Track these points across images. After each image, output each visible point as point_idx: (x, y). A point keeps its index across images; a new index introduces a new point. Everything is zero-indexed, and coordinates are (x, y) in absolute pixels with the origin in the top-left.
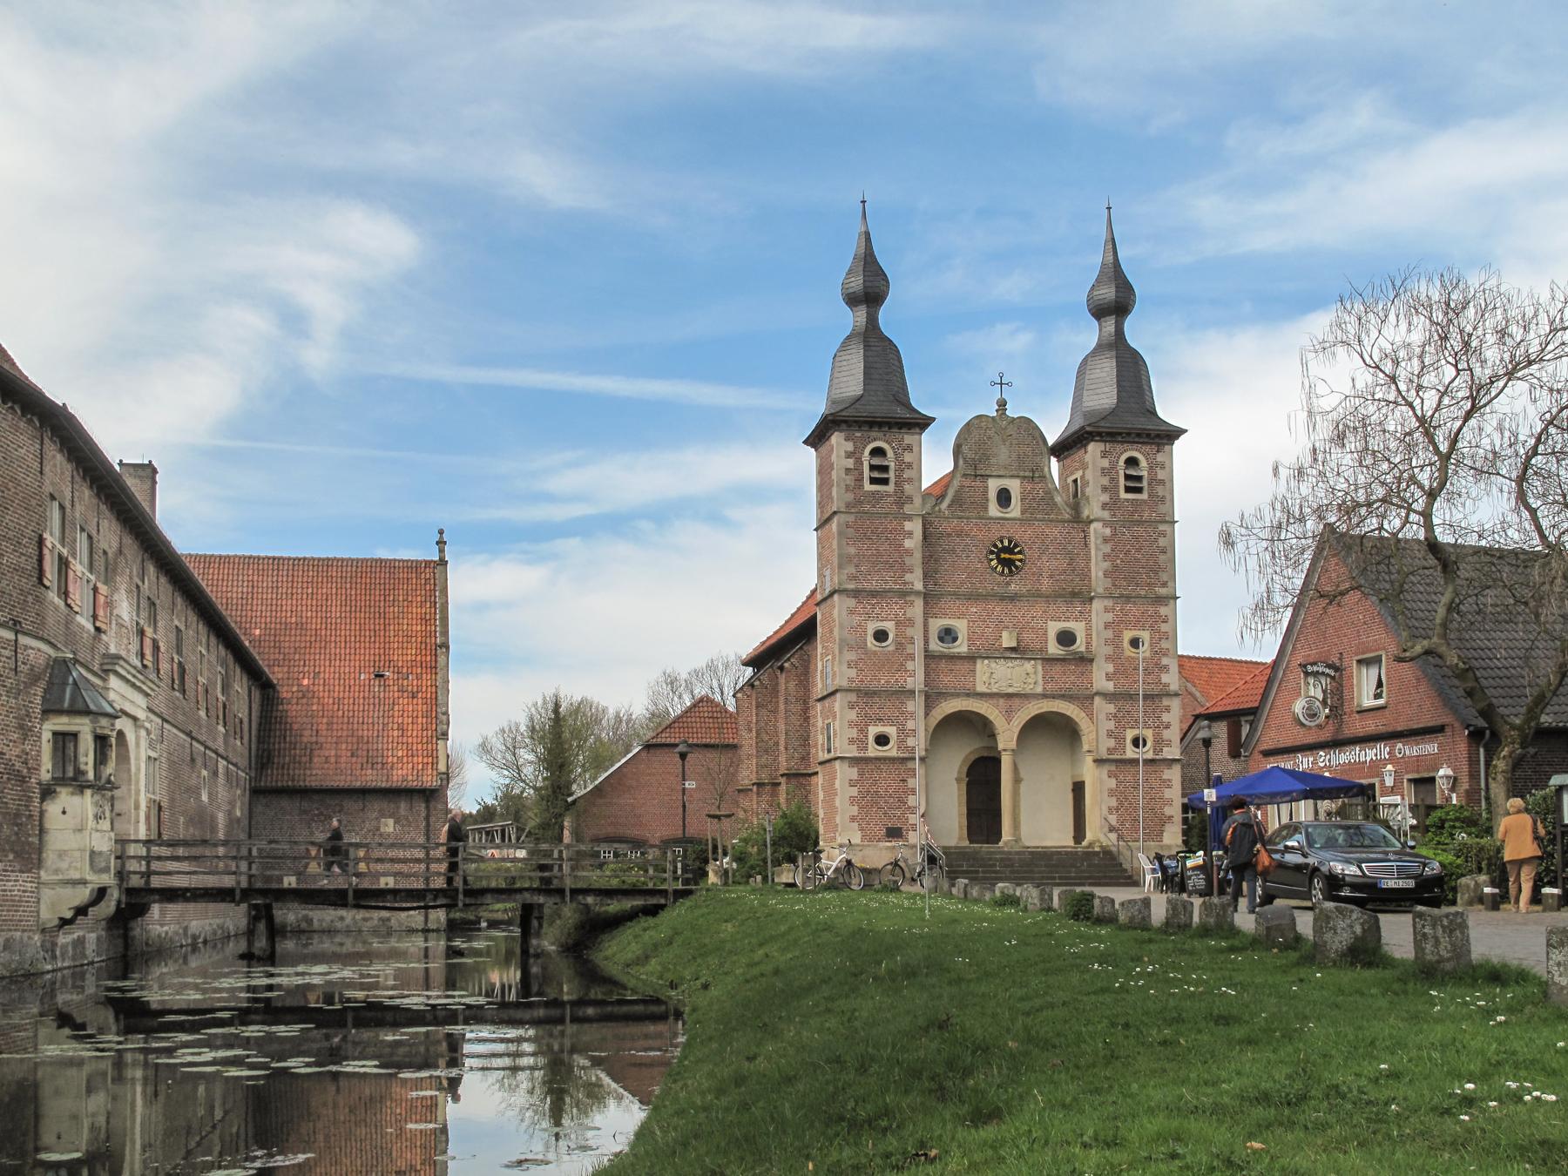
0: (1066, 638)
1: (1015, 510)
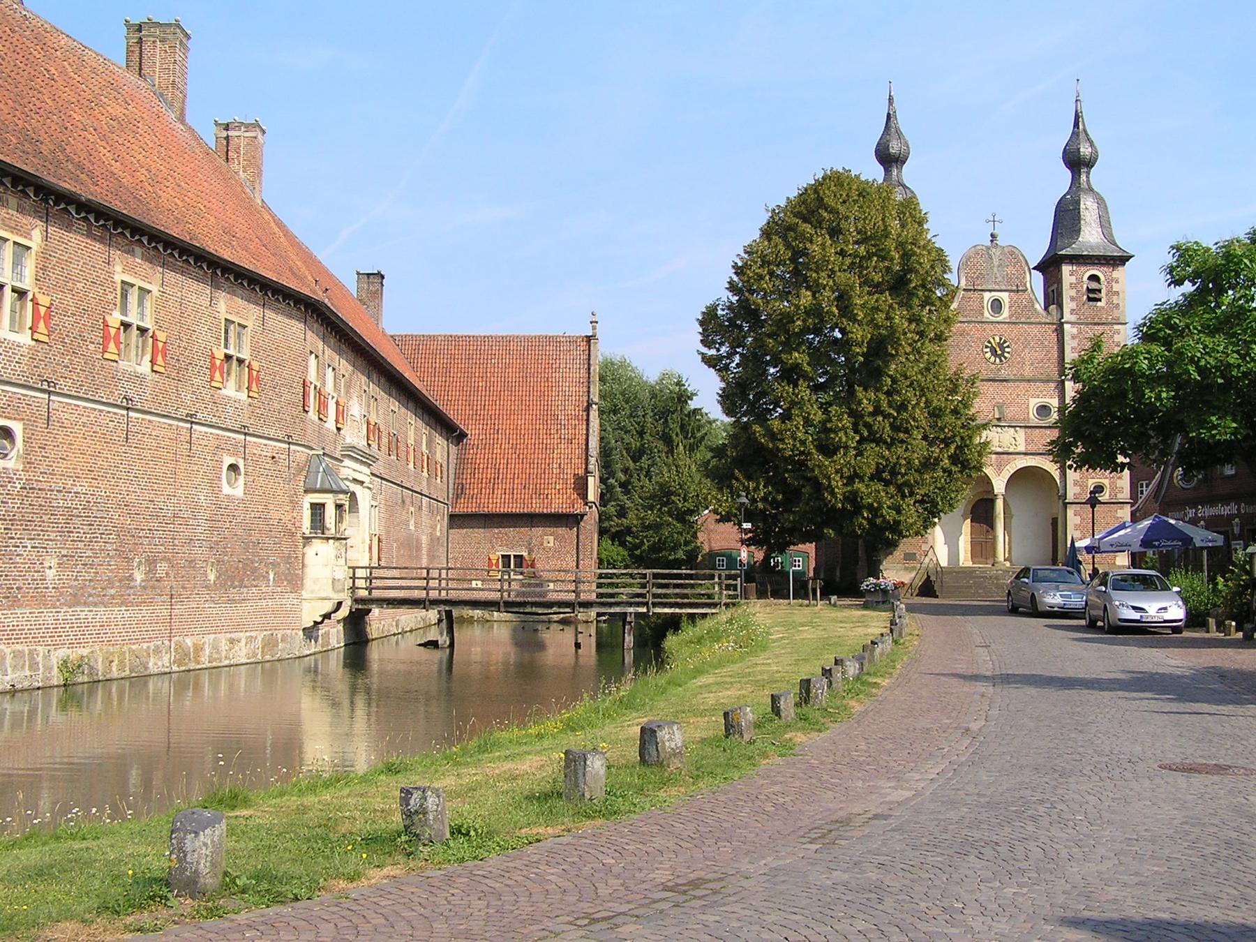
1: (1005, 314)
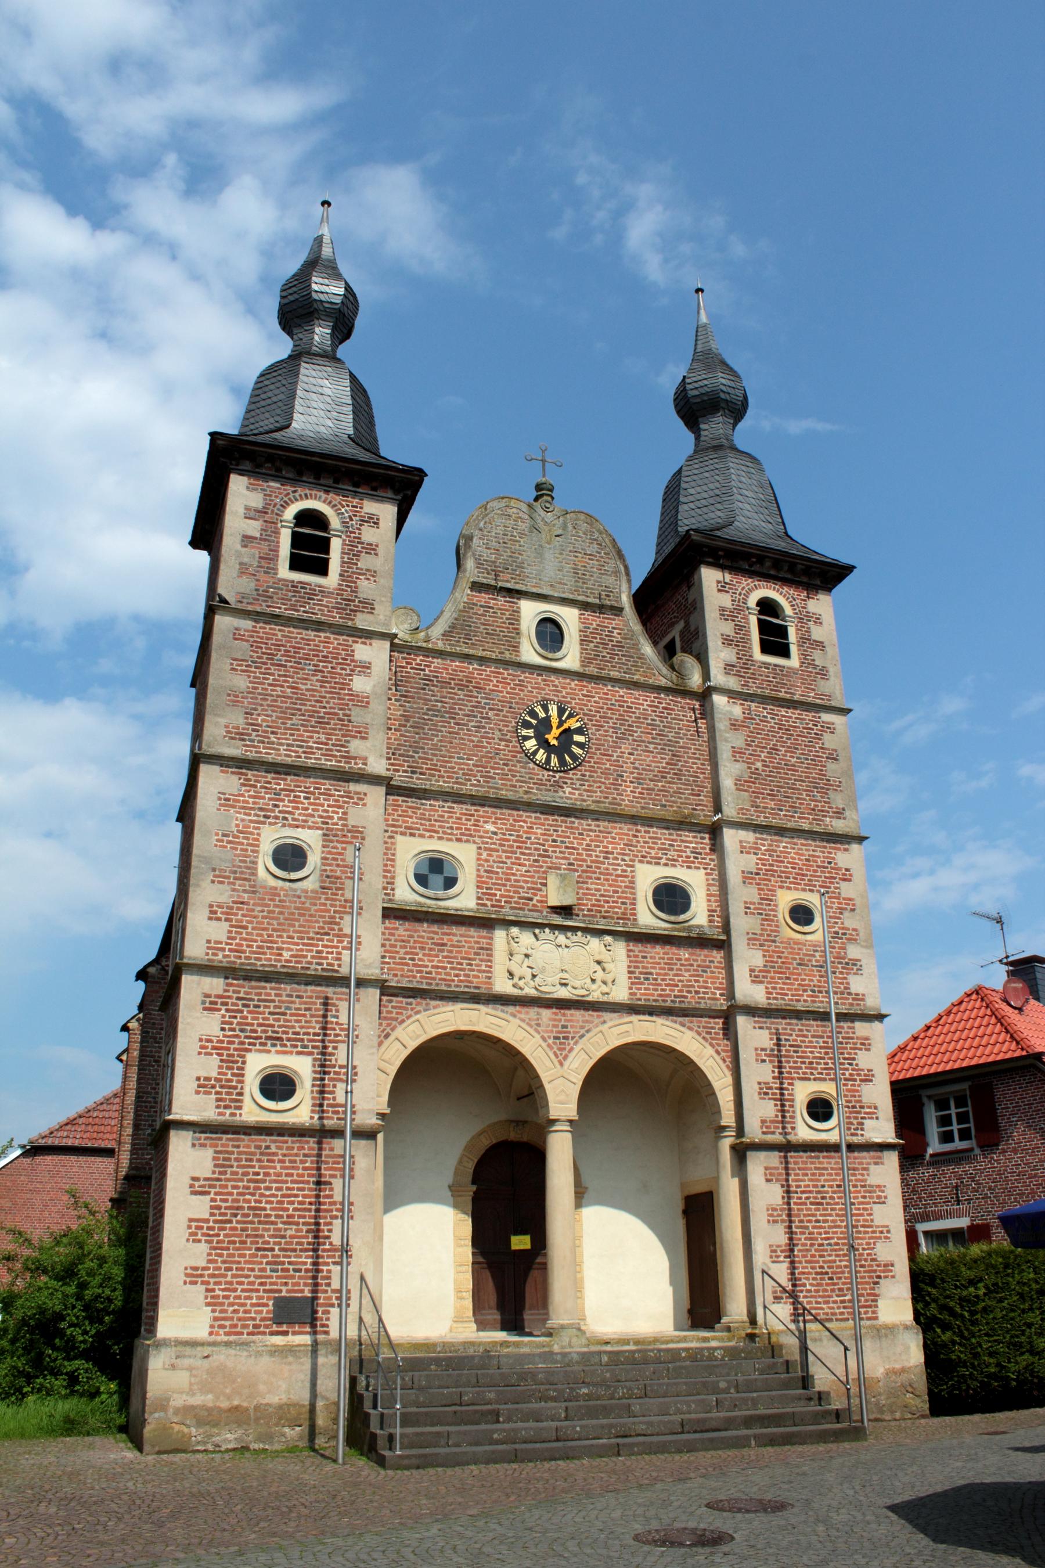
0: (671, 898)
1: (570, 657)
